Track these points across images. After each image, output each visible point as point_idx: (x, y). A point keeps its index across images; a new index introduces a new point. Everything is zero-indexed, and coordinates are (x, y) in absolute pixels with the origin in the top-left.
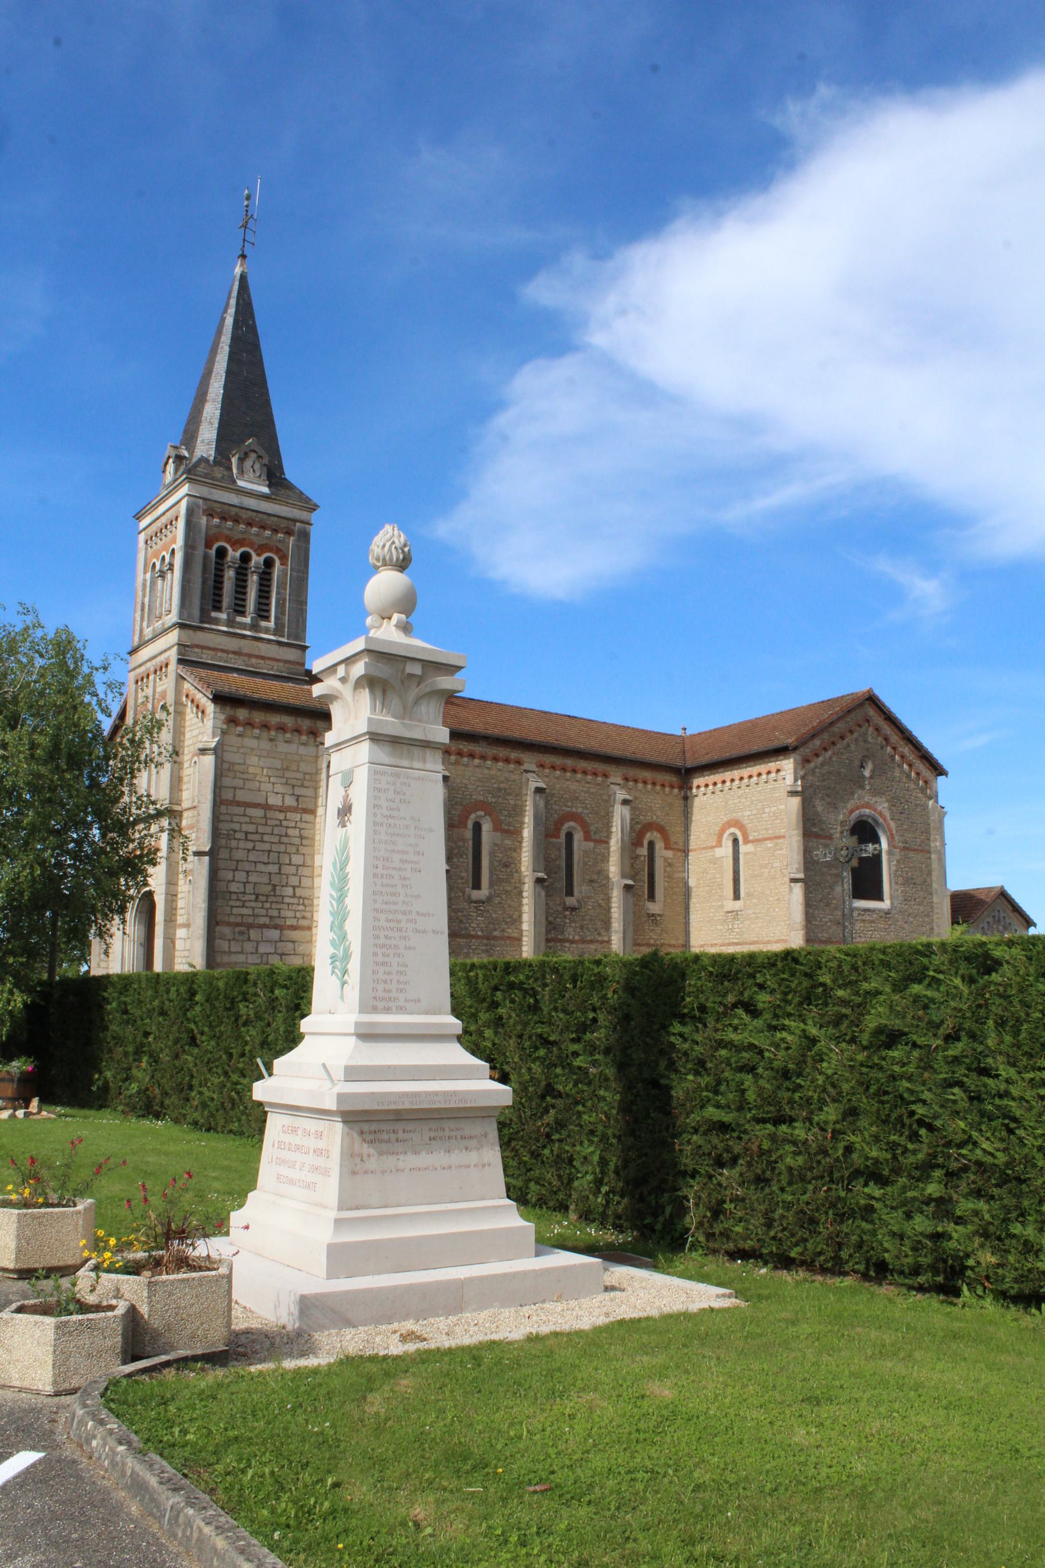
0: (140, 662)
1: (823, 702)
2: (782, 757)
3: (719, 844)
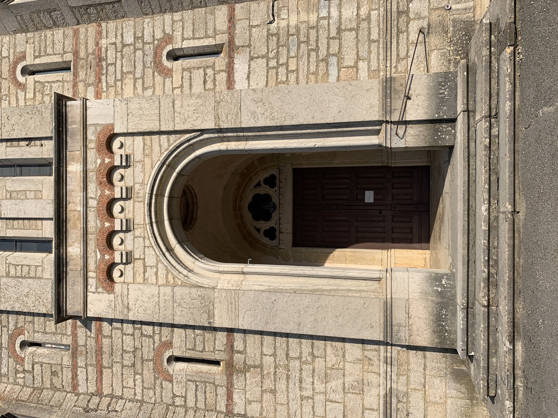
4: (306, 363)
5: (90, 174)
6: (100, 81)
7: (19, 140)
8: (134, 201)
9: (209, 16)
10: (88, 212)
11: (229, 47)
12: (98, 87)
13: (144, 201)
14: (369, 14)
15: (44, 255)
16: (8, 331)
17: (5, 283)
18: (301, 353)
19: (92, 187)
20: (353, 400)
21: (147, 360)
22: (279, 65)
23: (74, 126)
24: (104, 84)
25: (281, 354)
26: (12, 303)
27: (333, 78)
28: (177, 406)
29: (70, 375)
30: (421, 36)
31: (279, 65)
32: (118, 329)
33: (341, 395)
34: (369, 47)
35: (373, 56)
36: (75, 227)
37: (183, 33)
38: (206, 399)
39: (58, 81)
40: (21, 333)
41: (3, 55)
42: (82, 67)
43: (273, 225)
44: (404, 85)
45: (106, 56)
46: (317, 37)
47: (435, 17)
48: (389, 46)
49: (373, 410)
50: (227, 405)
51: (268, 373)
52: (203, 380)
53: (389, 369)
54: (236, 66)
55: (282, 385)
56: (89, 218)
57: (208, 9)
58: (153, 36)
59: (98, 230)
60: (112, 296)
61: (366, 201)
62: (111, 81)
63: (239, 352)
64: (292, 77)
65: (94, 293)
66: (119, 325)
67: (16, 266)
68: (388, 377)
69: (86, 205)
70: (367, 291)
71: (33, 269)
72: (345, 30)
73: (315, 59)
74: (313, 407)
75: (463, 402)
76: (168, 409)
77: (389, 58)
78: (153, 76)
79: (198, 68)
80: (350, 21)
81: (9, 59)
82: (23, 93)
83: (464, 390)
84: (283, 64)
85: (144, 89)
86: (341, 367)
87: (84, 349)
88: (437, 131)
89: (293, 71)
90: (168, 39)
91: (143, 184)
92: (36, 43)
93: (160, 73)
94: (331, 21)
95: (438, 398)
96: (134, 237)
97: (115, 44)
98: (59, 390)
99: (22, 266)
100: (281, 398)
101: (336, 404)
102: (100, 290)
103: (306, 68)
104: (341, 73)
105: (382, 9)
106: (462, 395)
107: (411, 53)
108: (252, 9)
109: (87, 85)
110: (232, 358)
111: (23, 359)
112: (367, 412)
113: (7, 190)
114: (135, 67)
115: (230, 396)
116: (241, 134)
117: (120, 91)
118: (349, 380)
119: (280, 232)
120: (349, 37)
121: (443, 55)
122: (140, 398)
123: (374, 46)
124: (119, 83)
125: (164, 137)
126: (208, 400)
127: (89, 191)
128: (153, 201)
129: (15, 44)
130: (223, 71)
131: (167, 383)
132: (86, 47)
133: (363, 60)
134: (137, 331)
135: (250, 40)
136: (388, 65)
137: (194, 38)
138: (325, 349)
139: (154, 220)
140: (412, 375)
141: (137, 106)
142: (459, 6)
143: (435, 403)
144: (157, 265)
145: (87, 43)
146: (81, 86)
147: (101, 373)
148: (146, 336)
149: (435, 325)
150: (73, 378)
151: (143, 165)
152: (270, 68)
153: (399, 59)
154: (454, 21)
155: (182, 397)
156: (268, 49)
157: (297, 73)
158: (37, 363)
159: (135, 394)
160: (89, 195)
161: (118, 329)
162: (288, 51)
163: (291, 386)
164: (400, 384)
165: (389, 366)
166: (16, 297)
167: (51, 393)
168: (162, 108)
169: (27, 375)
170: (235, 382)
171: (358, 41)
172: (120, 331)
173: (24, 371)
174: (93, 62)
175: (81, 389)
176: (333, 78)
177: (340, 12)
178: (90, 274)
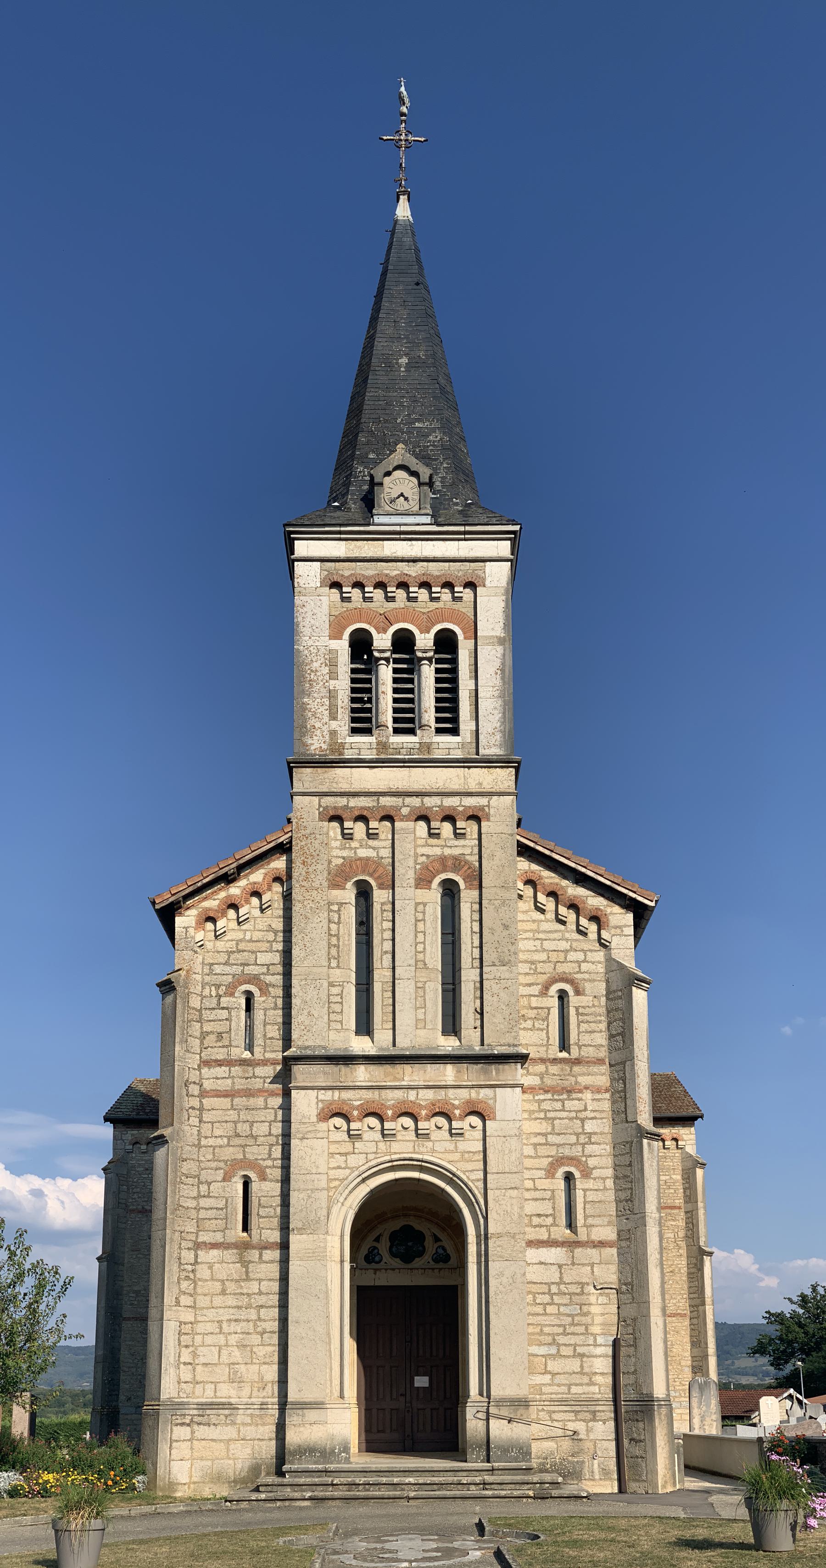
4: (255, 1326)
5: (442, 1092)
6: (546, 1092)
7: (482, 998)
9: (606, 1220)
12: (540, 1089)
13: (414, 1153)
14: (595, 1384)
15: (354, 1028)
16: (263, 974)
18: (265, 1321)
19: (429, 1095)
20: (223, 1372)
21: (244, 1151)
23: (494, 1073)
24: (542, 1097)
25: (262, 1300)
26: (300, 994)
27: (535, 1349)
28: (198, 1187)
29: (220, 1057)
30: (571, 1433)
31: (552, 1295)
32: (276, 1116)
33: (226, 1361)
34: (564, 1385)
35: (555, 1389)
36: (386, 1075)
37: (591, 1190)
38: (209, 1219)
39: (548, 1038)
40: (264, 991)
41: (582, 964)
42: (562, 1070)
45: (573, 1099)
46: (577, 1334)
47: (588, 1445)
49: (215, 1392)
50: (204, 1243)
51: (242, 1287)
52: (229, 1216)
53: (256, 1407)
54: (553, 1249)
55: (231, 1301)
56: (396, 1091)
57: (614, 1218)
58: (590, 1156)
61: (416, 1378)
62: (546, 1106)
63: (261, 1255)
64: (539, 1309)
65: (317, 1098)
66: (280, 1118)
67: (341, 995)
68: (248, 1406)
70: (331, 1386)
71: (339, 1018)
72: (582, 1361)
73: (556, 1332)
74: (212, 1333)
75: (231, 1474)
76: (195, 1177)
77: (552, 1403)
78: (548, 1156)
79: (554, 1208)
82: (537, 993)
83: (243, 1474)
85: (535, 1145)
86: (254, 1361)
87: (251, 1075)
88: (480, 1447)
89: (545, 1310)
90: (587, 1174)
91: (433, 1151)
92: (593, 1009)
93: (551, 1164)
95: (233, 1452)
96: (377, 1142)
97: (586, 1109)
98: (202, 1043)
99: (341, 1003)
100: (218, 1301)
101: (217, 1357)
102: (321, 1105)
103: (547, 1323)
105: (599, 1396)
106: (237, 1473)
107: (556, 1424)
108: (610, 1266)
110: (254, 1248)
111: (232, 995)
112: (213, 1386)
113: (425, 982)
114: (559, 1134)
115: (214, 1246)
116: (483, 1259)
117: (533, 1117)
118: (242, 1368)
120: (574, 1365)
121: (552, 1453)
122: (202, 1143)
123: (564, 1389)
124: (542, 1115)
125: (481, 1175)
126: (209, 1222)
127: (425, 1091)
128: (415, 1163)
129: (594, 980)
130: (550, 1235)
131: (222, 1175)
132: (584, 1074)
133: (552, 1379)
134: (274, 1139)
135: (579, 1264)
136: (546, 1403)
137: (585, 1203)
138: (270, 1344)
140: (253, 1428)
141: (513, 1148)
142: (596, 1466)
143: (228, 1450)
146: (541, 1068)
148: (270, 1150)
150: (216, 1061)
151: (452, 1152)
152: (549, 1286)
153: (550, 1413)
154: (583, 1462)
155: (209, 1193)
157: (542, 1314)
158: (230, 1013)
159: (206, 1137)
160: (420, 1091)
161: (276, 1116)
162: (565, 1305)
163: (232, 1311)
166: (308, 999)
167: (198, 1034)
168: (510, 1175)
169: (215, 1001)
170: (230, 1251)
171: (571, 1374)
172: (273, 1118)
173: (219, 996)
175: (205, 1071)
176: (535, 1349)
177: (600, 1356)
178: (337, 1093)
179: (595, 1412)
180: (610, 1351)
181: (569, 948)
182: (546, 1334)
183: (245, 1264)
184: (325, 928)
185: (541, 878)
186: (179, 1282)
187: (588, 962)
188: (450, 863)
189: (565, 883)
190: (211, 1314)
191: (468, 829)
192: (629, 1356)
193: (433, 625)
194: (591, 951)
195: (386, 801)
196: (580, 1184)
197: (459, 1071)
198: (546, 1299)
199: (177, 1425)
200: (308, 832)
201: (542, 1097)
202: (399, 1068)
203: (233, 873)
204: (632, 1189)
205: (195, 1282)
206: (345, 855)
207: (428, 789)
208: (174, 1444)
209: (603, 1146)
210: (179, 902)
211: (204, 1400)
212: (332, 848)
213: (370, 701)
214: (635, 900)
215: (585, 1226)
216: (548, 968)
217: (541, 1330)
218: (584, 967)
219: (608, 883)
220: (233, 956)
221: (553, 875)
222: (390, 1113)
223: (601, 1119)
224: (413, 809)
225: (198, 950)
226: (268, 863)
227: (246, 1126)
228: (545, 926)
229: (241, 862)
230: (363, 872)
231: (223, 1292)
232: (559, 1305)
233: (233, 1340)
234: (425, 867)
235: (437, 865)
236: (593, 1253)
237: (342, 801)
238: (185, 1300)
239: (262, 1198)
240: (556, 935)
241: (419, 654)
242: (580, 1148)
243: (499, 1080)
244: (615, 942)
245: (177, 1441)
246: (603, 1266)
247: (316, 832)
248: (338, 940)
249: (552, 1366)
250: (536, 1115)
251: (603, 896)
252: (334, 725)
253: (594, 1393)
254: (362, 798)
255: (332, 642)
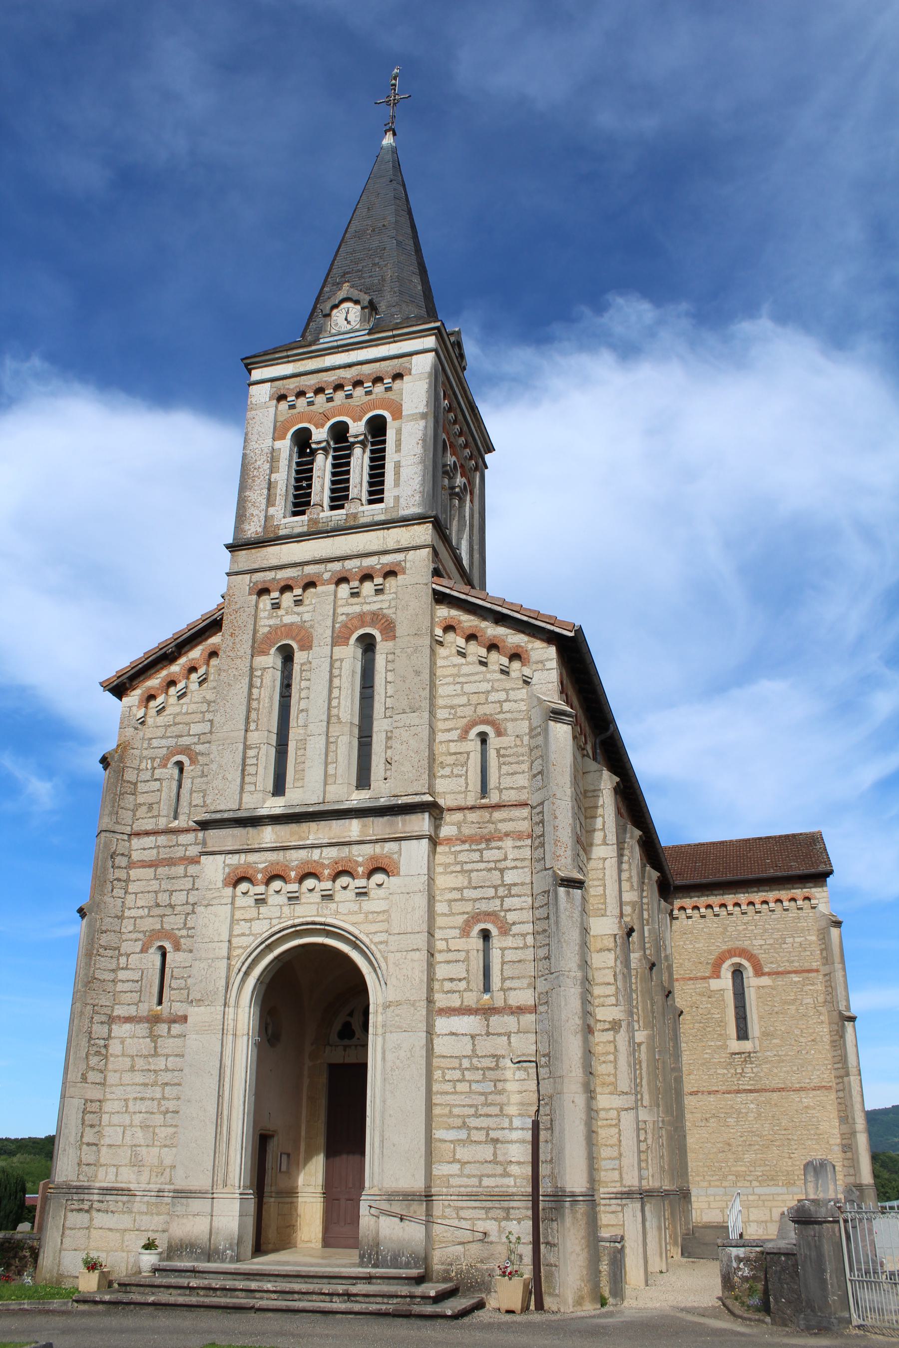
0: (266, 564)
1: (760, 839)
2: (811, 885)
3: (716, 974)
4: (159, 1103)
5: (346, 849)
6: (464, 842)
8: (318, 903)
10: (306, 850)
11: (489, 1009)
12: (457, 839)
13: (318, 916)
14: (509, 1176)
15: (270, 787)
16: (195, 744)
17: (237, 749)
18: (168, 1099)
19: (333, 852)
20: (125, 1155)
22: (463, 1070)
23: (400, 825)
24: (458, 848)
28: (118, 960)
31: (463, 1070)
33: (129, 1143)
34: (474, 1176)
35: (464, 1181)
37: (510, 948)
38: (126, 992)
39: (467, 784)
40: (193, 761)
43: (357, 1036)
44: (414, 1215)
45: (492, 849)
46: (491, 1116)
48: (473, 1198)
49: (117, 1176)
50: (119, 1017)
51: (149, 1063)
52: (143, 989)
53: (153, 1194)
54: (466, 1018)
55: (139, 1078)
56: (301, 851)
58: (510, 910)
59: (287, 863)
60: (220, 884)
62: (462, 857)
63: (169, 1029)
67: (257, 757)
68: (146, 1193)
69: (313, 847)
72: (495, 1148)
73: (466, 1113)
76: (115, 949)
77: (460, 1198)
79: (468, 971)
80: (505, 1154)
81: (499, 713)
84: (463, 1075)
85: (450, 901)
89: (455, 1088)
90: (505, 930)
91: (337, 912)
92: (515, 750)
93: (467, 922)
94: (507, 1131)
97: (505, 859)
99: (257, 765)
100: (127, 1078)
102: (227, 870)
103: (457, 1103)
104: (448, 1144)
105: (514, 1190)
109: (459, 825)
110: (164, 1022)
111: (165, 766)
113: (338, 737)
114: (475, 888)
115: (128, 1019)
117: (449, 870)
119: (345, 1048)
120: (487, 1152)
121: (458, 1258)
123: (474, 1181)
124: (458, 868)
127: (329, 849)
129: (516, 720)
130: (462, 1002)
133: (461, 1169)
134: (190, 907)
135: (493, 1034)
136: (453, 1198)
137: (503, 963)
139: (298, 928)
144: (253, 935)
145: (511, 820)
146: (458, 816)
147: (150, 866)
149: (187, 1242)
151: (356, 913)
153: (458, 1209)
156: (482, 1057)
157: (452, 1093)
158: (161, 784)
159: (130, 909)
160: (324, 849)
162: (478, 1082)
163: (138, 1088)
164: (139, 1204)
165: (156, 1194)
167: (132, 807)
168: (412, 936)
169: (149, 773)
170: (141, 1025)
171: (482, 1163)
173: (154, 769)
174: (485, 831)
177: (516, 1142)
178: (243, 856)
179: (508, 1209)
180: (528, 1135)
181: (490, 688)
182: (455, 1116)
183: (154, 1038)
184: (246, 694)
185: (460, 622)
186: (87, 1058)
187: (510, 701)
188: (368, 618)
189: (484, 624)
190: (119, 1092)
191: (387, 585)
192: (546, 1141)
193: (365, 413)
194: (513, 689)
195: (310, 569)
196: (496, 941)
197: (364, 826)
198: (457, 1075)
199: (72, 1211)
200: (238, 606)
201: (458, 848)
202: (305, 826)
203: (172, 652)
204: (549, 944)
205: (106, 1057)
206: (271, 623)
207: (349, 552)
208: (67, 1232)
209: (523, 899)
210: (125, 683)
211: (105, 1185)
212: (261, 618)
213: (310, 486)
214: (553, 632)
215: (502, 989)
216: (468, 711)
217: (450, 1112)
218: (506, 706)
219: (525, 618)
220: (169, 730)
221: (472, 618)
222: (293, 874)
223: (522, 868)
224: (334, 573)
225: (139, 726)
226: (206, 639)
227: (166, 896)
228: (465, 670)
229: (179, 641)
230: (287, 636)
231: (132, 1069)
232: (470, 1081)
233: (137, 1119)
234: (345, 625)
235: (356, 622)
236: (510, 1022)
237: (270, 575)
238: (92, 1076)
239: (175, 970)
240: (477, 678)
241: (351, 440)
242: (498, 902)
243: (405, 832)
244: (537, 678)
245: (71, 1229)
246: (522, 1035)
247: (246, 605)
248: (259, 703)
249: (463, 1153)
250: (452, 868)
251: (523, 632)
252: (271, 511)
253: (508, 1186)
254: (289, 570)
255: (276, 443)
